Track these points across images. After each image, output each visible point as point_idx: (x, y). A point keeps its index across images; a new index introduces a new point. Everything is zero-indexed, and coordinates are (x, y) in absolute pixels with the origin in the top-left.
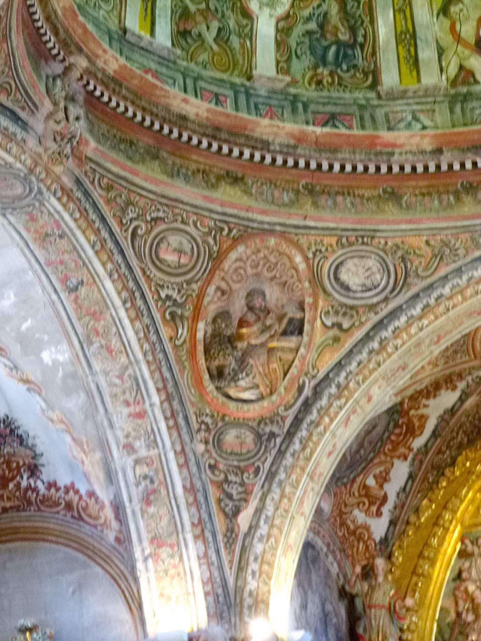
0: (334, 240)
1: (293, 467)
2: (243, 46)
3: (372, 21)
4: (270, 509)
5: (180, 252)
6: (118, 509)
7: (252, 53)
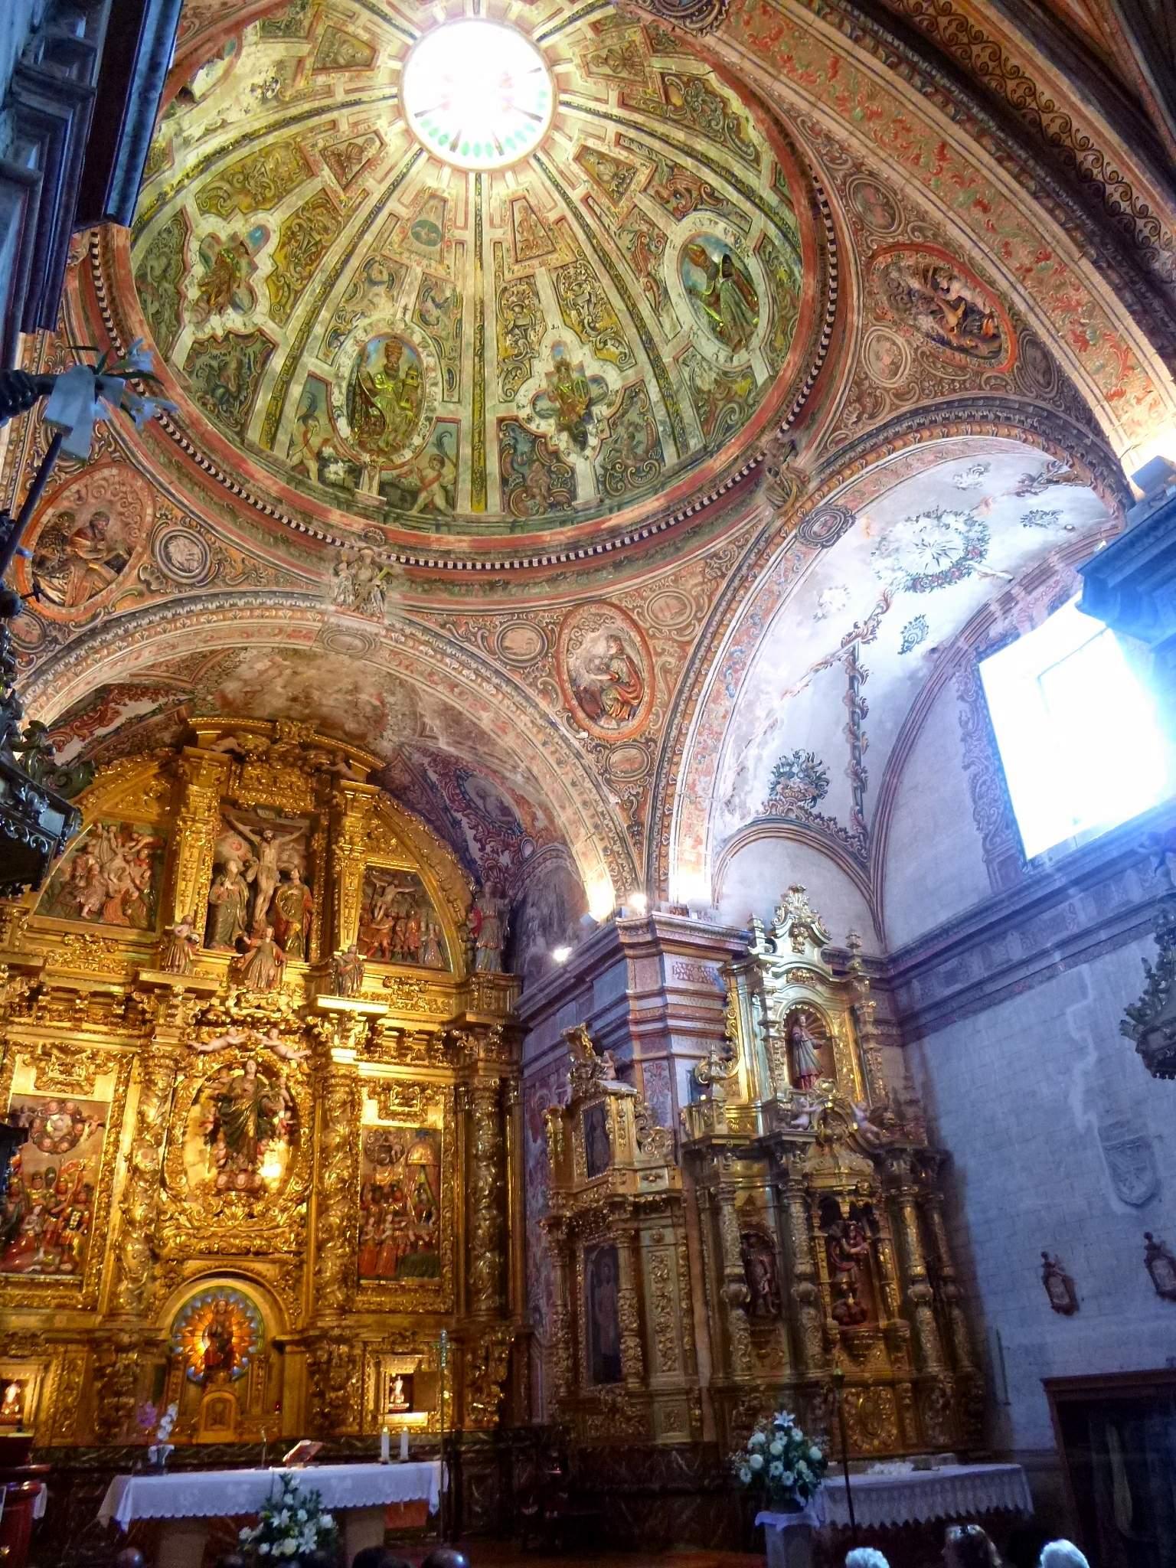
0: (180, 515)
1: (62, 674)
3: (255, 391)
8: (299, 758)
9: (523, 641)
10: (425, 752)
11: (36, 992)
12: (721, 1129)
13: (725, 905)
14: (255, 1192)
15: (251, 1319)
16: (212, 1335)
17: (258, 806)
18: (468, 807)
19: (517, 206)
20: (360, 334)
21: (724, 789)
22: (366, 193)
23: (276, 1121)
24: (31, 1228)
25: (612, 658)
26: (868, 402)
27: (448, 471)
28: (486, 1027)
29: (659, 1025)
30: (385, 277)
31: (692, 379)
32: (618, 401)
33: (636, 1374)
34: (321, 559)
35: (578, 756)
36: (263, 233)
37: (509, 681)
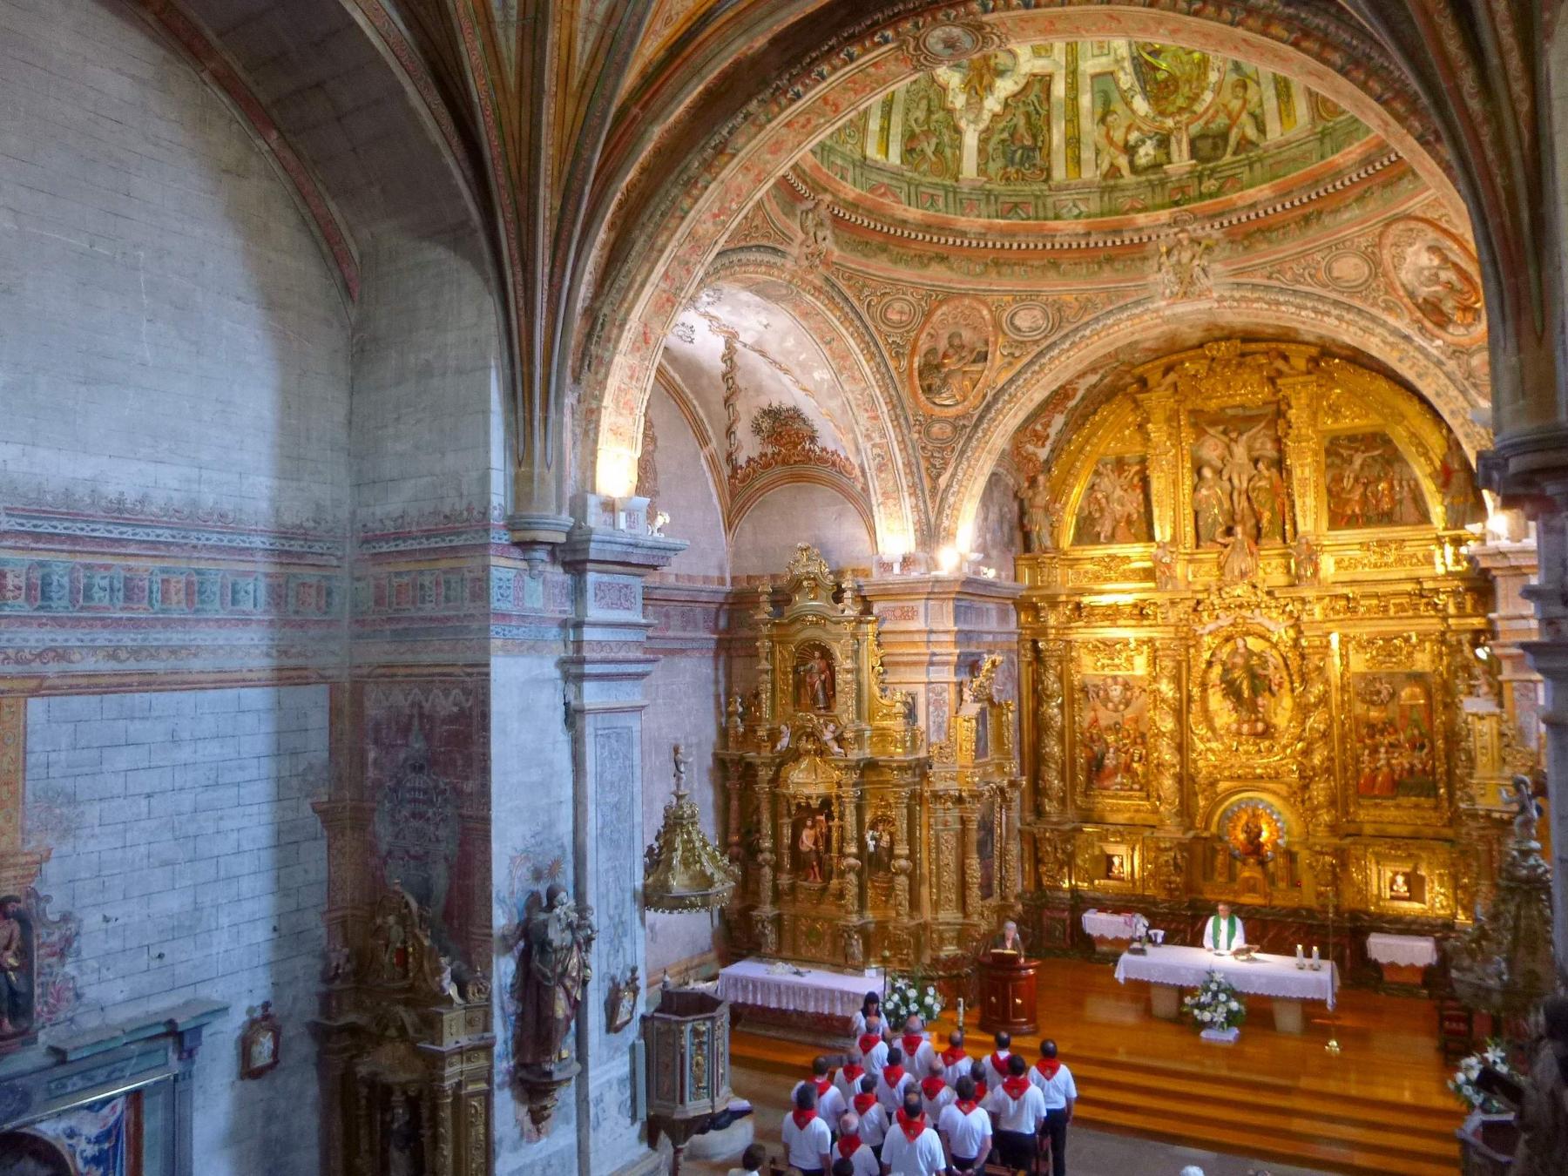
2: (954, 154)
3: (1049, 130)
4: (960, 474)
5: (901, 313)
7: (959, 160)
9: (1350, 268)
14: (1268, 732)
24: (1110, 762)
25: (1439, 268)
34: (1145, 259)
35: (1439, 364)
37: (1350, 308)
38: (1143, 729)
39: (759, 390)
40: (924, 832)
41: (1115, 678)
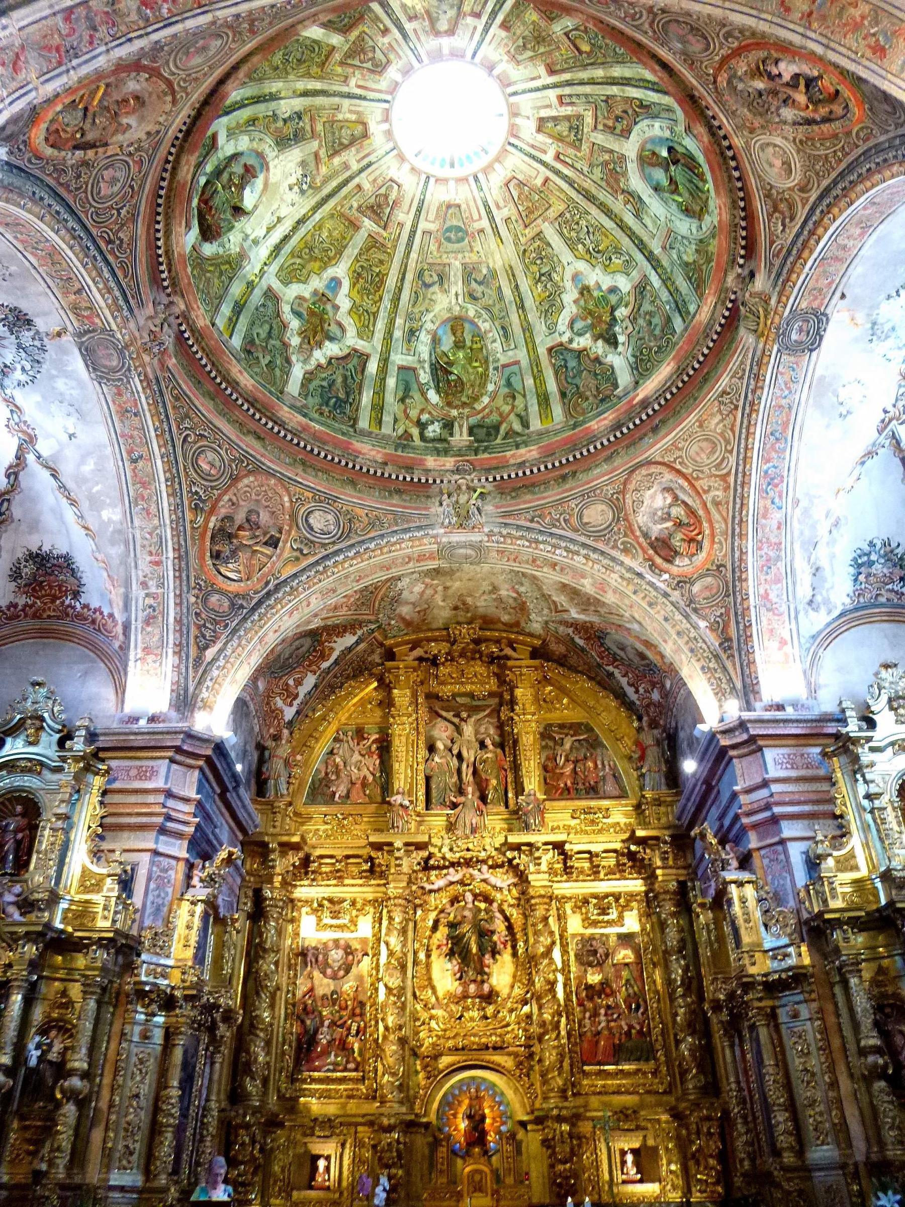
4: (229, 651)
5: (212, 465)
6: (126, 627)
7: (286, 382)
8: (473, 651)
9: (597, 514)
10: (567, 624)
11: (306, 861)
12: (837, 904)
13: (822, 694)
14: (489, 997)
15: (500, 1103)
16: (470, 1117)
17: (454, 696)
18: (615, 660)
19: (511, 186)
20: (429, 326)
21: (804, 591)
22: (401, 225)
23: (495, 938)
24: (323, 1039)
25: (670, 506)
26: (783, 206)
27: (519, 402)
28: (656, 838)
29: (767, 814)
30: (436, 278)
31: (680, 257)
32: (632, 300)
33: (791, 1148)
34: (428, 497)
35: (666, 595)
36: (336, 283)
37: (595, 550)
38: (361, 998)
39: (34, 526)
40: (113, 1046)
41: (336, 942)
